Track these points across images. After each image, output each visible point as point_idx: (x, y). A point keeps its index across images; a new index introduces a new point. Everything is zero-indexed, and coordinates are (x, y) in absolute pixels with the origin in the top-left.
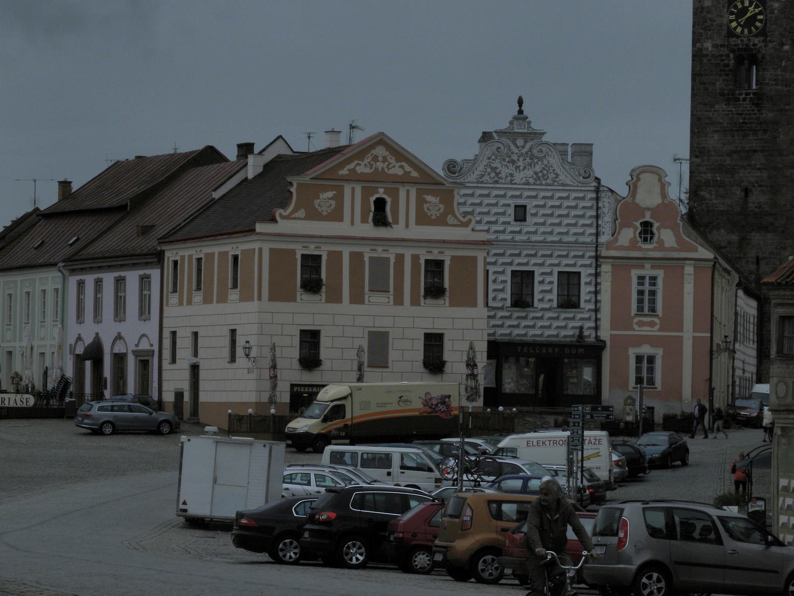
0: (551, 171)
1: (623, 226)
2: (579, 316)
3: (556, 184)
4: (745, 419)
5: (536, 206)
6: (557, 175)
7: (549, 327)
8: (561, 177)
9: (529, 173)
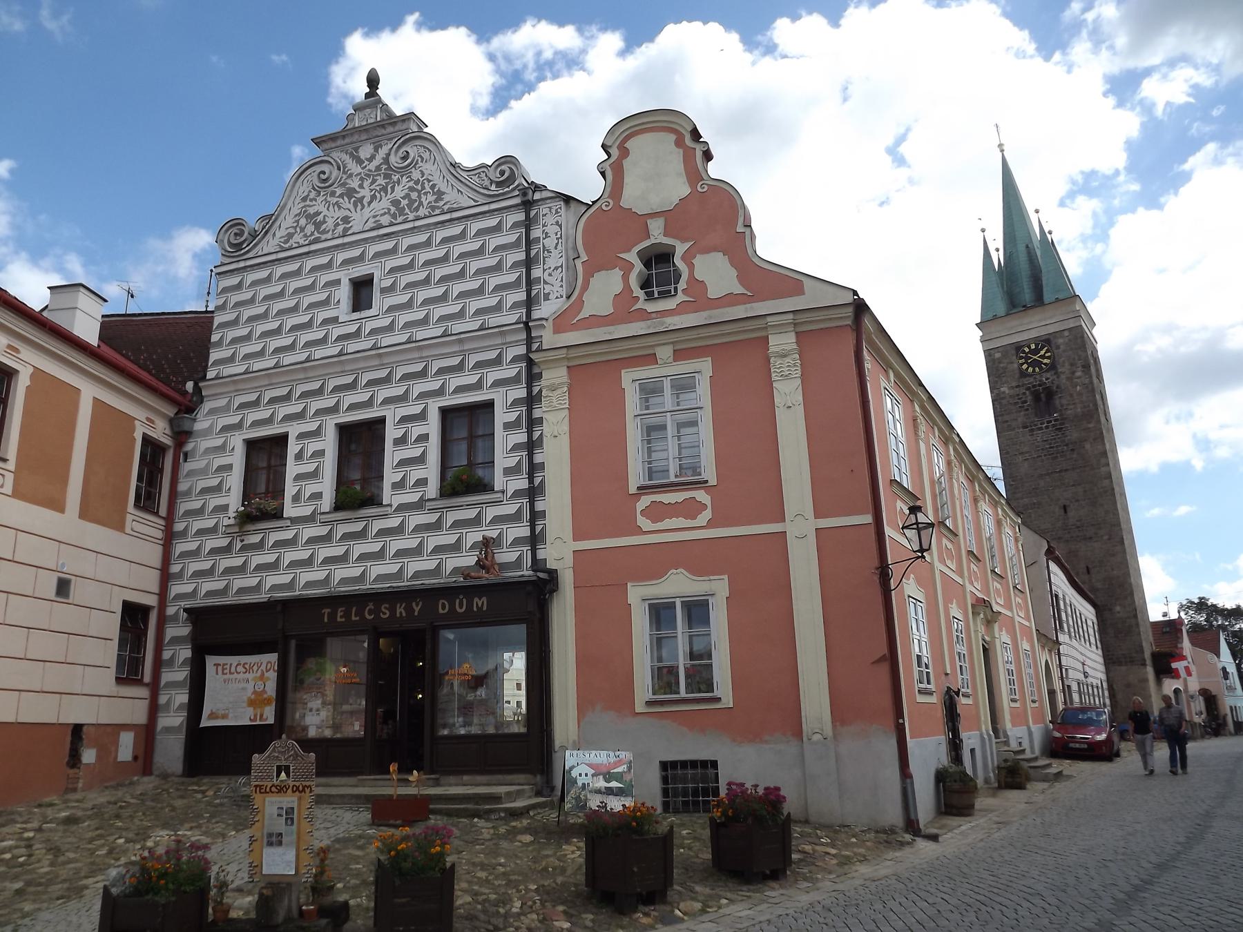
0: (428, 189)
1: (592, 269)
2: (491, 512)
3: (437, 212)
4: (1086, 746)
5: (392, 270)
6: (440, 195)
7: (417, 551)
8: (446, 198)
9: (385, 203)
